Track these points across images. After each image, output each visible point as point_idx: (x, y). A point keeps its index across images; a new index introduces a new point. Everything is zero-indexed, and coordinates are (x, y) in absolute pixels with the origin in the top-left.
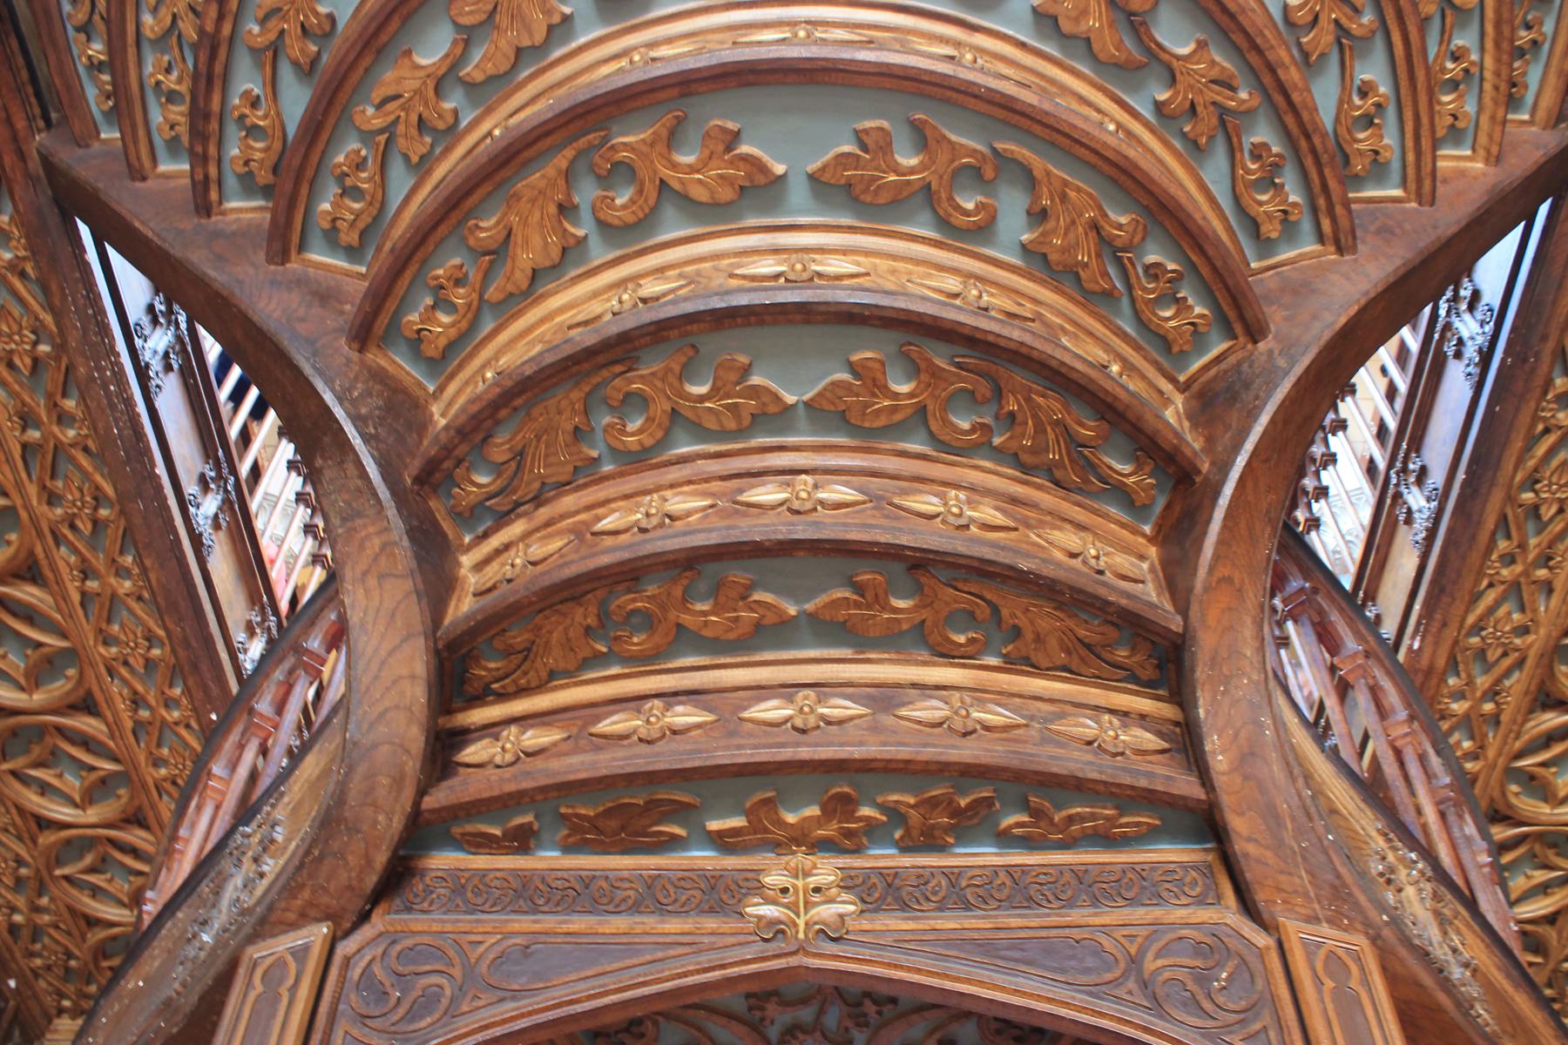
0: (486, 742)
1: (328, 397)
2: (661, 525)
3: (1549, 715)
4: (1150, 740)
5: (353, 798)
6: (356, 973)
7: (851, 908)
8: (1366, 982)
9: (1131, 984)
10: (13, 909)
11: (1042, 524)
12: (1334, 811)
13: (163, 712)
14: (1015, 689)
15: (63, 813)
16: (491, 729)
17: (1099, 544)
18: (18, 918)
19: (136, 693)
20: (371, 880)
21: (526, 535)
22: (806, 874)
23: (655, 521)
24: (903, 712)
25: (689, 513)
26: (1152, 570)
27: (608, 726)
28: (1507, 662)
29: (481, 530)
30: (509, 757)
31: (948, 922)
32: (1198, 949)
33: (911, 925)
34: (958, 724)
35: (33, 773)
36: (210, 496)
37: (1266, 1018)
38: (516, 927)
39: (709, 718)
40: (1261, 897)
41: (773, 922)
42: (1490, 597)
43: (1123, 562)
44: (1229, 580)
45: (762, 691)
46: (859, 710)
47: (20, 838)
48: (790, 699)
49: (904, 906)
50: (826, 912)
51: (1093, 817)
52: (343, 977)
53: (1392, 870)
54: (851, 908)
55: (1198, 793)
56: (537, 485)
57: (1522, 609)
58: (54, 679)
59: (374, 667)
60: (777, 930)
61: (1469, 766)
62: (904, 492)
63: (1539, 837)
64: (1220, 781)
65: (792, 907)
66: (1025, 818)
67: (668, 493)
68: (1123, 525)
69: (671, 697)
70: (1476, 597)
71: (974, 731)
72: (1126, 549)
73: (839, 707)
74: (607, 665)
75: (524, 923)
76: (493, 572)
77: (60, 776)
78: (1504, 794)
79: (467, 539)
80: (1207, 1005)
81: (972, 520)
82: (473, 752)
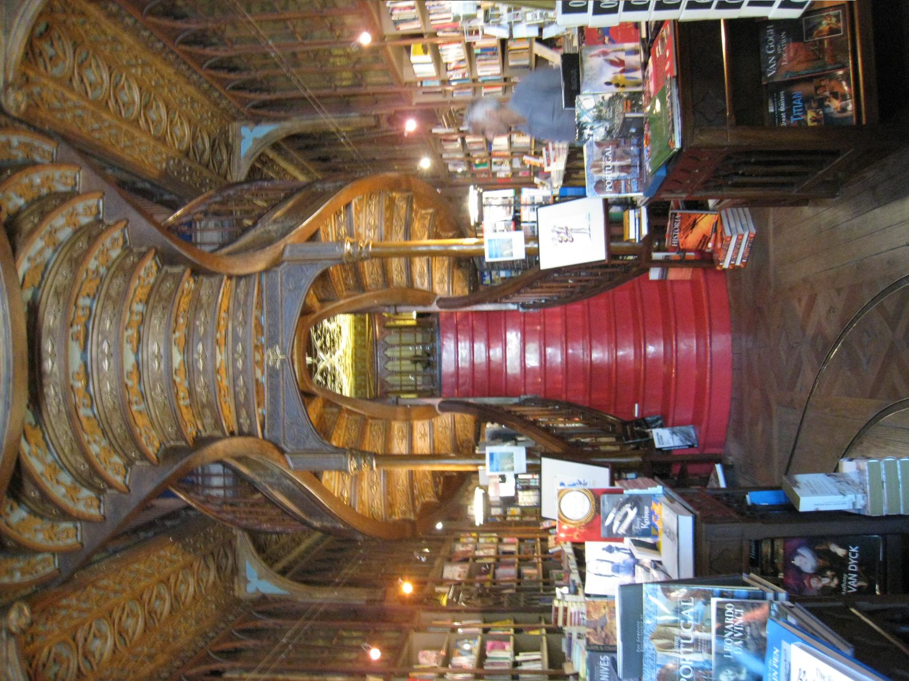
4: (243, 282)
12: (253, 241)
15: (191, 589)
16: (240, 425)
27: (242, 398)
50: (278, 351)
60: (283, 362)
62: (199, 333)
75: (281, 414)
82: (246, 429)
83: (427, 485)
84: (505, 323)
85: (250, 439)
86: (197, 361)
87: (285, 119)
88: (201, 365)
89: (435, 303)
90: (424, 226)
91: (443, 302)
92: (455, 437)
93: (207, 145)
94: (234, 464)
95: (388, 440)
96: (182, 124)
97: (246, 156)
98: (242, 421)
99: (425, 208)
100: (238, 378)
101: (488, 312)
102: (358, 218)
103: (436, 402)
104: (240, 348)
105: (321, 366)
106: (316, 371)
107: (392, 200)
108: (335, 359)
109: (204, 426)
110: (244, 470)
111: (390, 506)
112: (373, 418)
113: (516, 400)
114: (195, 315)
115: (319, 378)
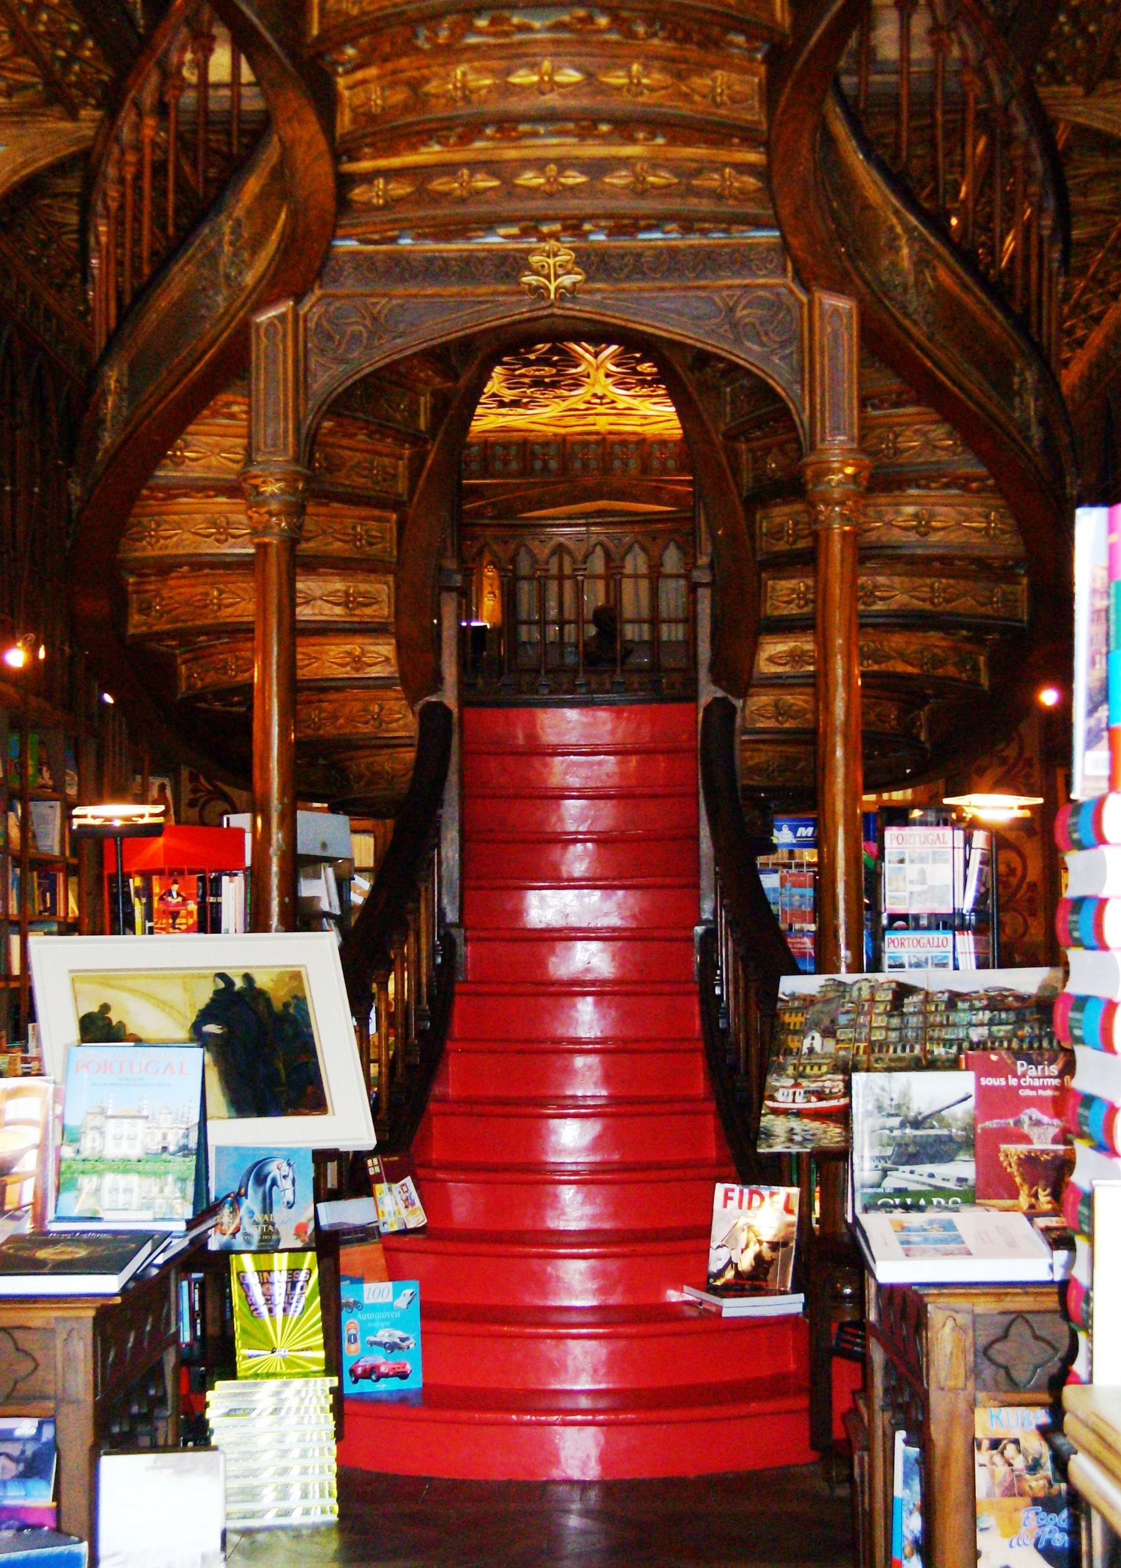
1: (254, 19)
4: (751, 182)
6: (311, 325)
7: (579, 277)
9: (727, 327)
16: (368, 178)
21: (379, 77)
22: (556, 255)
25: (480, 89)
27: (439, 185)
30: (381, 201)
39: (495, 183)
40: (805, 276)
41: (538, 288)
45: (527, 164)
46: (581, 179)
49: (609, 275)
50: (567, 280)
52: (306, 329)
53: (897, 237)
54: (579, 277)
60: (539, 292)
62: (608, 69)
65: (547, 277)
69: (474, 166)
75: (400, 290)
80: (764, 339)
81: (646, 87)
82: (358, 193)
83: (225, 669)
84: (662, 887)
85: (330, 206)
86: (534, 67)
88: (522, 77)
89: (720, 694)
90: (938, 662)
91: (722, 712)
92: (350, 745)
94: (271, 155)
95: (342, 566)
98: (381, 182)
99: (991, 664)
100: (495, 175)
101: (696, 838)
102: (947, 486)
103: (449, 697)
104: (574, 178)
107: (1010, 578)
108: (604, 386)
109: (363, 82)
110: (253, 185)
111: (165, 567)
112: (401, 525)
113: (452, 916)
114: (657, 57)
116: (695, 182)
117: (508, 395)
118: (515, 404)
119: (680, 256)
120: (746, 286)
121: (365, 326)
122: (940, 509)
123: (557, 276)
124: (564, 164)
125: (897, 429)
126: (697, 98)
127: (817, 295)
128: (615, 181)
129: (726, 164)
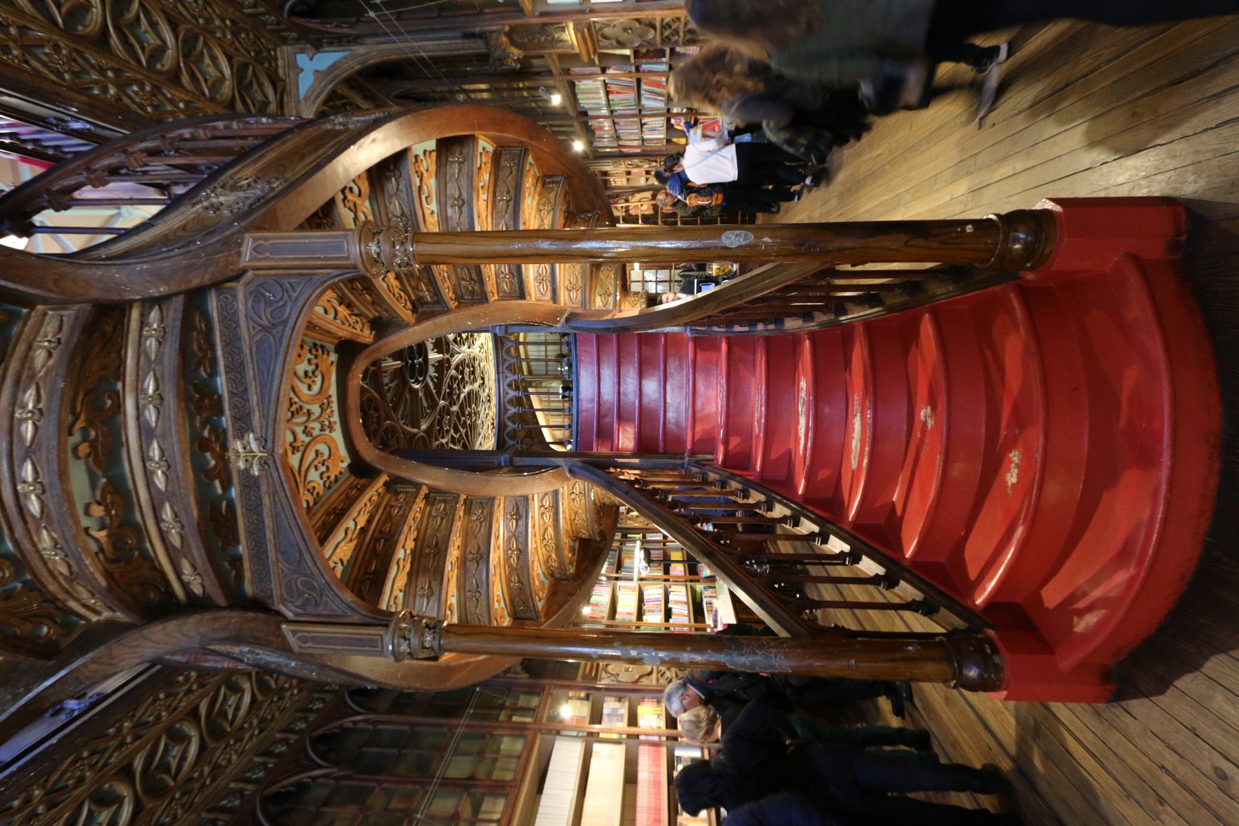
0: (192, 587)
2: (61, 549)
3: (112, 42)
4: (154, 315)
5: (226, 634)
6: (299, 611)
7: (251, 436)
8: (266, 239)
9: (275, 331)
10: (292, 694)
11: (31, 368)
12: (184, 228)
13: (192, 679)
14: (134, 374)
15: (247, 699)
16: (185, 585)
17: (39, 339)
18: (296, 692)
19: (184, 695)
20: (261, 615)
23: (59, 552)
24: (153, 425)
25: (52, 538)
26: (52, 310)
27: (176, 540)
28: (80, 60)
29: (76, 619)
30: (198, 577)
31: (254, 399)
32: (256, 301)
33: (257, 414)
34: (157, 402)
35: (230, 717)
36: (66, 706)
37: (285, 281)
38: (274, 558)
40: (230, 274)
41: (260, 464)
42: (34, 63)
43: (50, 327)
44: (55, 281)
45: (149, 484)
46: (155, 445)
47: (260, 708)
48: (153, 473)
49: (249, 415)
51: (198, 340)
53: (212, 206)
54: (251, 436)
55: (181, 298)
56: (45, 605)
57: (43, 46)
58: (183, 731)
59: (161, 646)
60: (263, 463)
61: (148, 88)
62: (22, 439)
63: (186, 57)
64: (174, 289)
65: (253, 457)
66: (202, 369)
67: (40, 547)
68: (25, 324)
69: (158, 520)
70: (37, 73)
71: (159, 395)
72: (41, 322)
73: (155, 452)
74: (146, 549)
75: (272, 555)
76: (99, 606)
77: (230, 706)
78: (161, 73)
79: (83, 622)
80: (281, 303)
81: (34, 407)
82: (197, 590)
86: (26, 496)
87: (356, 40)
93: (227, 72)
96: (153, 25)
97: (307, 98)
98: (185, 578)
100: (162, 504)
105: (456, 359)
106: (449, 368)
115: (453, 372)
116: (153, 358)
117: (479, 381)
118: (483, 379)
119: (231, 366)
120: (246, 316)
121: (297, 579)
122: (449, 191)
123: (252, 451)
124: (144, 459)
125: (390, 215)
126: (51, 362)
127: (242, 264)
128: (154, 419)
129: (140, 336)
